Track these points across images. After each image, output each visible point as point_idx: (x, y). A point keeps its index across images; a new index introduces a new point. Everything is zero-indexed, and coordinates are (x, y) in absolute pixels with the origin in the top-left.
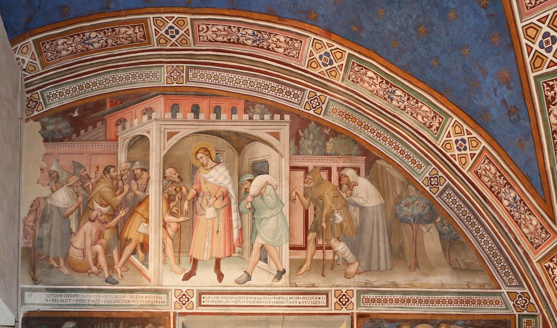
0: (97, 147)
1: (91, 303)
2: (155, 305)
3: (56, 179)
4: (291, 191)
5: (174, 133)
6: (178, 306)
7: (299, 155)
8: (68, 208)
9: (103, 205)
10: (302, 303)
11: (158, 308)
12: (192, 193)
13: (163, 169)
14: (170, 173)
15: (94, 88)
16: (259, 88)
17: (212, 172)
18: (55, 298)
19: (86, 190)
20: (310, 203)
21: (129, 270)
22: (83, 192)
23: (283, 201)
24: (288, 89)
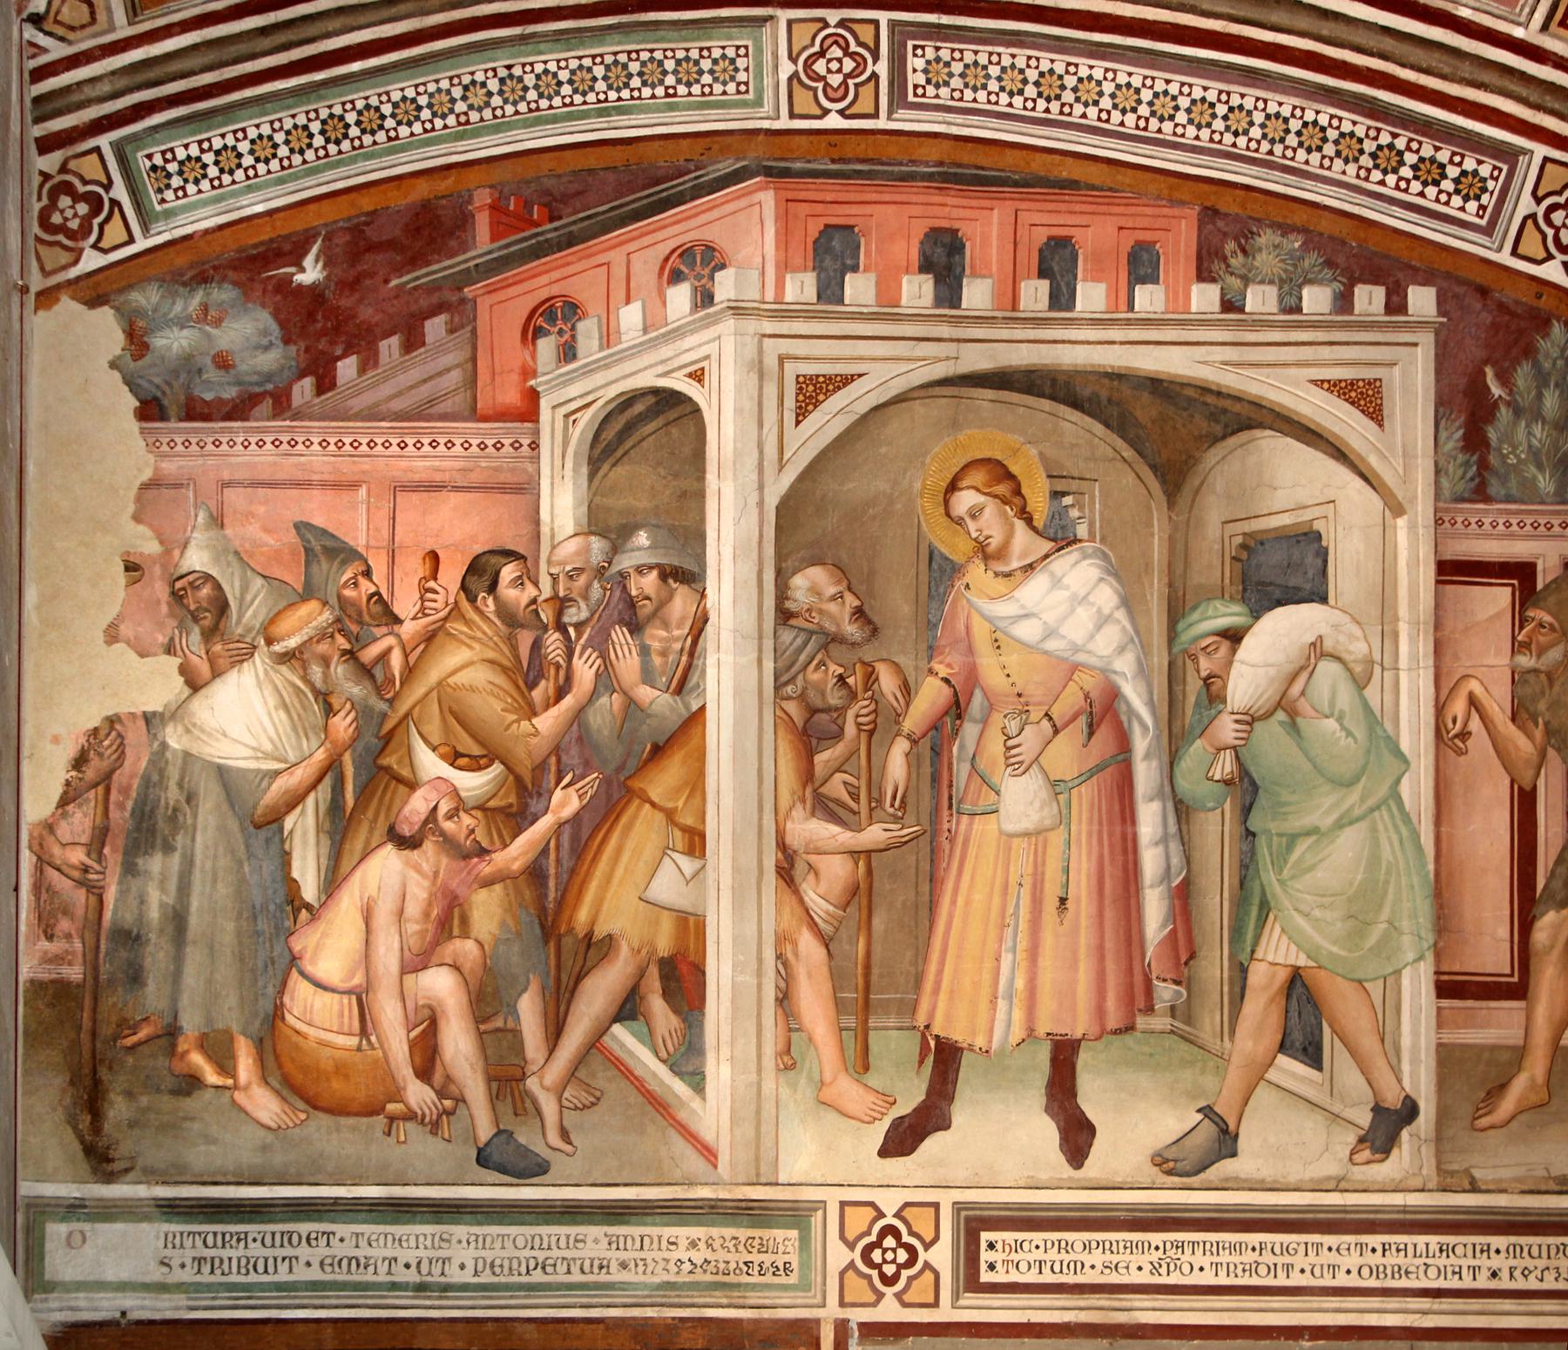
0: (427, 448)
1: (402, 1276)
2: (738, 1286)
3: (208, 621)
4: (1444, 692)
5: (829, 379)
6: (858, 1289)
7: (1487, 499)
8: (277, 773)
9: (462, 761)
10: (1505, 1274)
12: (930, 696)
13: (779, 572)
14: (814, 590)
15: (404, 131)
16: (1273, 141)
17: (1034, 590)
19: (372, 677)
20: (1543, 755)
21: (603, 1104)
22: (356, 690)
23: (1405, 745)
24: (1427, 151)
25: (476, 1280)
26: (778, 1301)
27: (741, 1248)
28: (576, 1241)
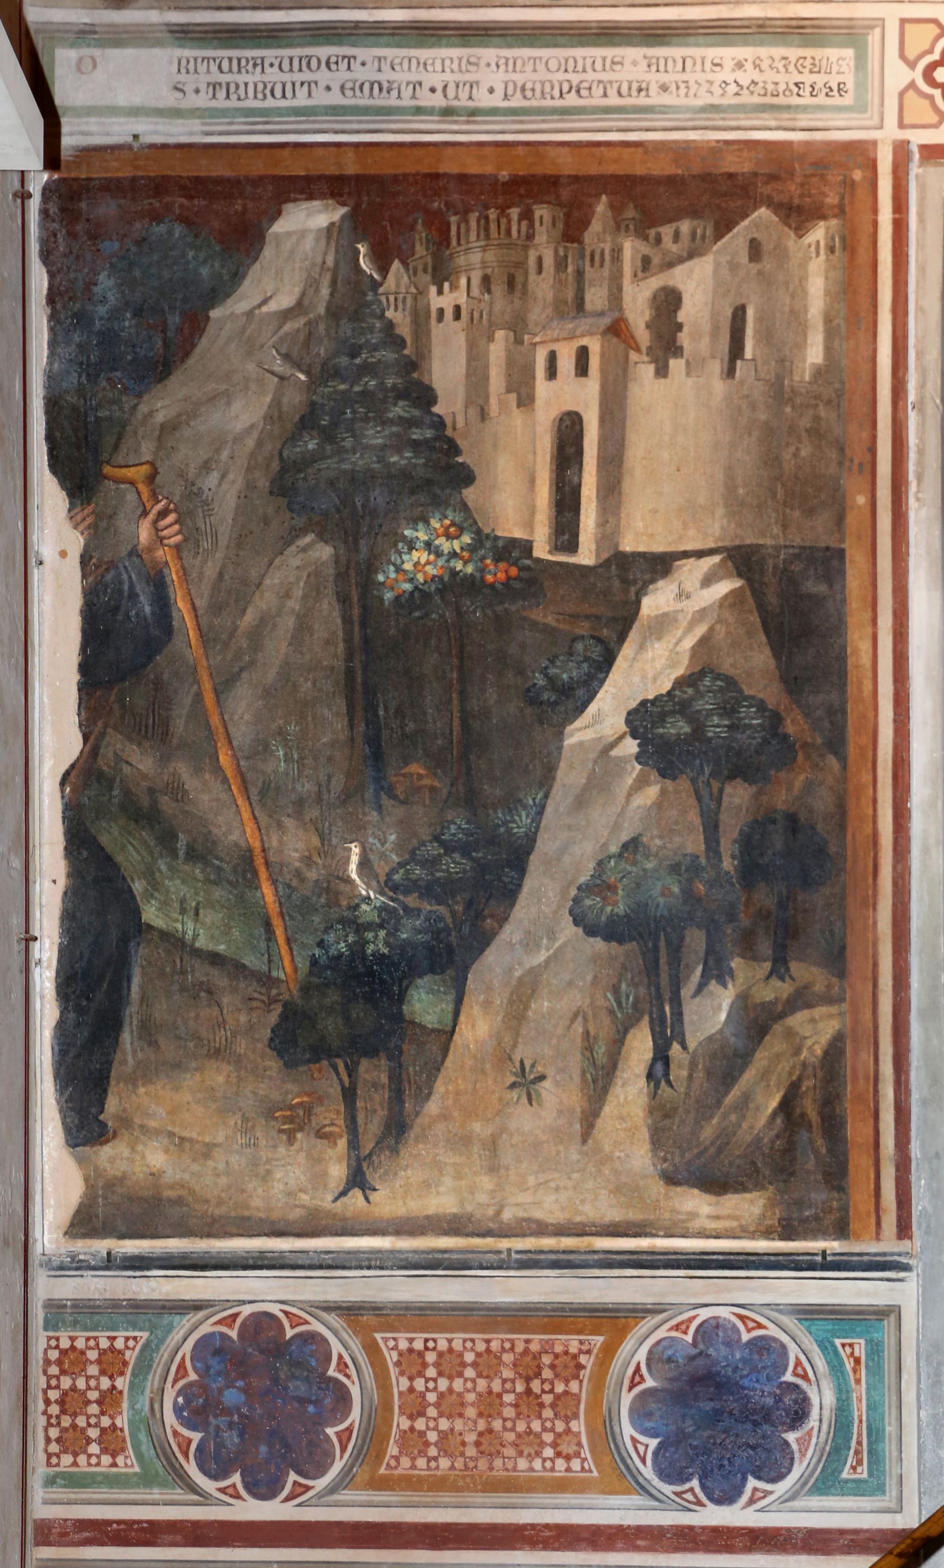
1: (427, 100)
2: (788, 108)
6: (918, 109)
11: (804, 120)
25: (506, 104)
27: (791, 68)
28: (613, 63)
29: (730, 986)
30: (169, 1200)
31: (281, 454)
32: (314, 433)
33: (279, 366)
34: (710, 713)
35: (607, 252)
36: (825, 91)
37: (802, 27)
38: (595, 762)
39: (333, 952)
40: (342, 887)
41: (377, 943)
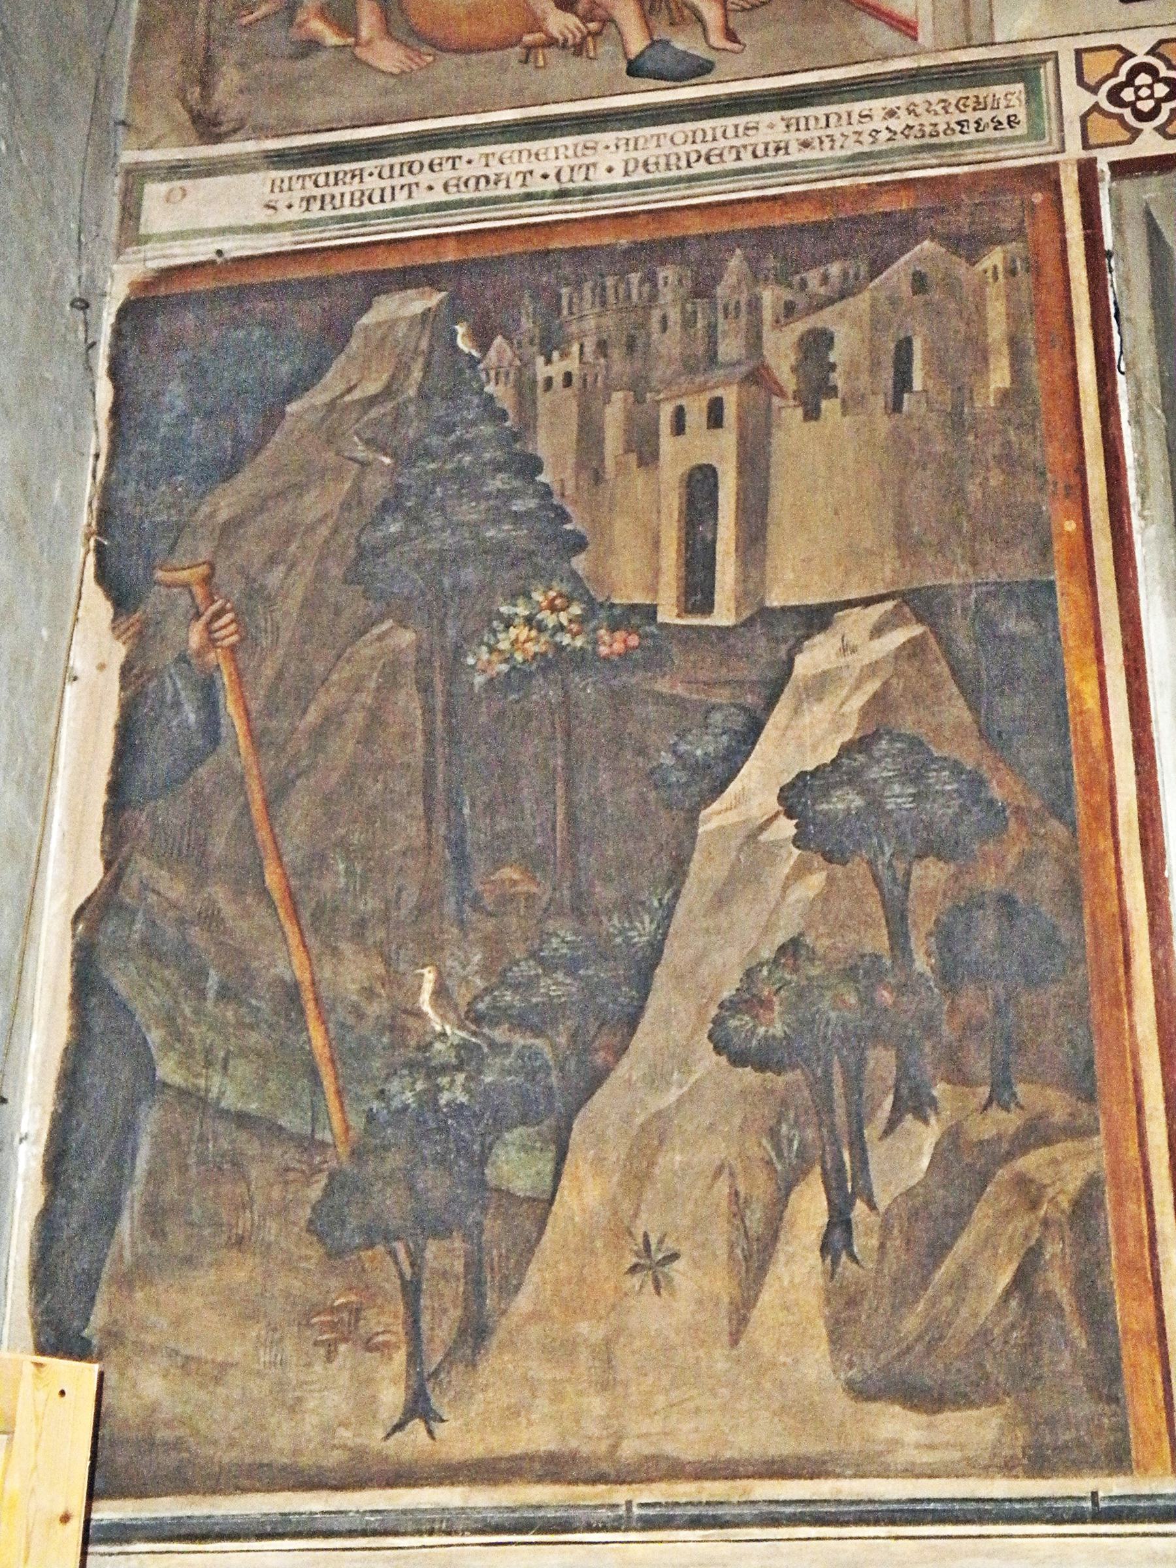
2: (951, 145)
18: (318, 192)
25: (627, 180)
26: (1002, 154)
27: (952, 109)
28: (747, 129)
29: (933, 1120)
30: (165, 1444)
31: (358, 539)
32: (399, 515)
33: (361, 452)
34: (888, 781)
35: (742, 304)
36: (992, 125)
37: (965, 70)
38: (740, 850)
39: (396, 1104)
40: (411, 1022)
41: (454, 1092)
